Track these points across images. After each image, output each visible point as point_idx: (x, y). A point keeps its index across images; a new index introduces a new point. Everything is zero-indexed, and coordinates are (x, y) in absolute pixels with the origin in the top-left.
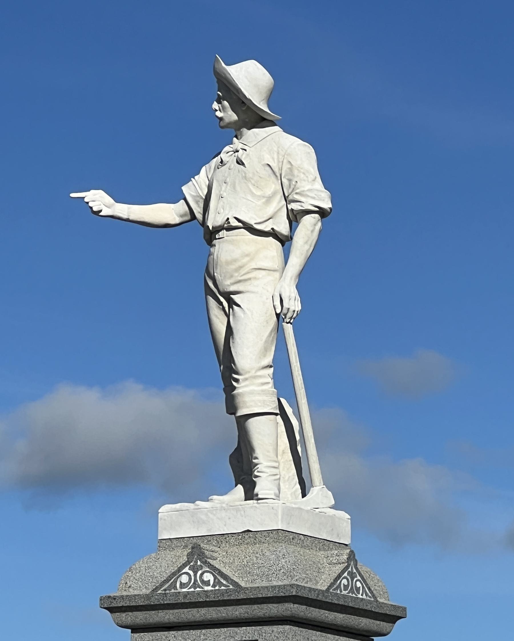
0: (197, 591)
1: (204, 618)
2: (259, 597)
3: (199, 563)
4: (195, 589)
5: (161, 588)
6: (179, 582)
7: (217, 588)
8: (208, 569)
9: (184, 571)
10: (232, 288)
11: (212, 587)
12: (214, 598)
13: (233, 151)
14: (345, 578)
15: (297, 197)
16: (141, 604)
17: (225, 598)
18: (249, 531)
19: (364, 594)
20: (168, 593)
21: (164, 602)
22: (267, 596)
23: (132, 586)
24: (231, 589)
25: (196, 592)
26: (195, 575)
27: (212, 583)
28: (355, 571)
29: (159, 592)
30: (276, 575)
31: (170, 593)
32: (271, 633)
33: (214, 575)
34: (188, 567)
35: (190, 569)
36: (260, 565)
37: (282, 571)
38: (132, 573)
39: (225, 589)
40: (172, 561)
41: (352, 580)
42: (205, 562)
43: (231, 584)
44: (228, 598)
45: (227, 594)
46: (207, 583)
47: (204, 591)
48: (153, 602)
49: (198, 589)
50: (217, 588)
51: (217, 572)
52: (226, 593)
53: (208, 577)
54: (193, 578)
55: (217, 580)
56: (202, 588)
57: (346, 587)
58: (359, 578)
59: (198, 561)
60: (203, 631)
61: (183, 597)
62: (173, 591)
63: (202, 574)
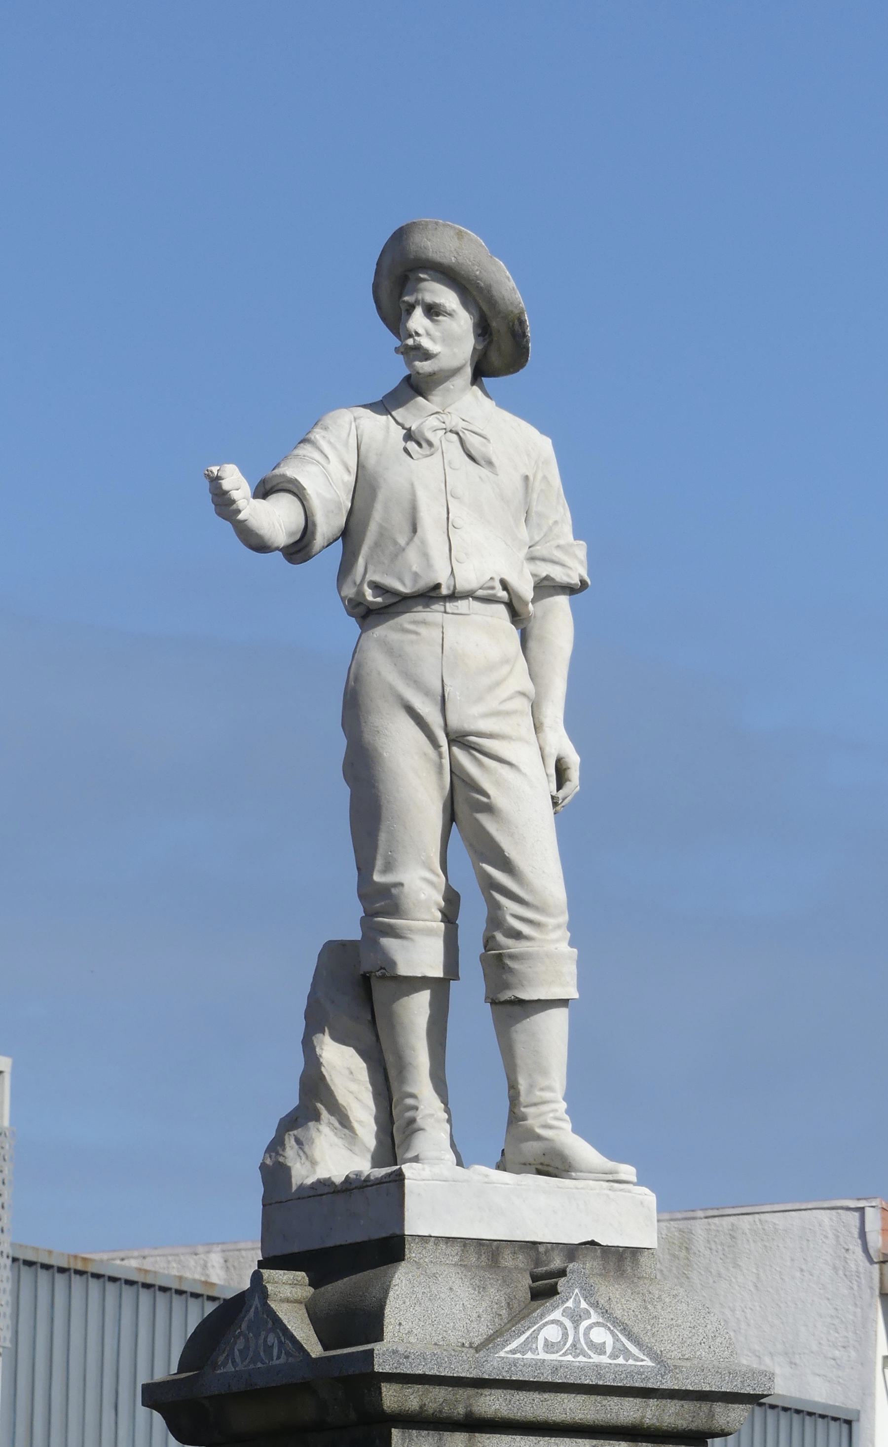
1: (569, 1418)
2: (704, 1389)
3: (584, 1305)
5: (504, 1346)
7: (621, 1361)
8: (601, 1320)
10: (483, 725)
11: (610, 1357)
12: (614, 1380)
13: (445, 429)
15: (558, 555)
16: (463, 1375)
17: (637, 1385)
18: (593, 1243)
21: (511, 1377)
22: (720, 1390)
25: (577, 1364)
27: (609, 1350)
29: (502, 1354)
30: (708, 1347)
31: (523, 1358)
34: (561, 1310)
35: (564, 1314)
37: (718, 1340)
42: (595, 1305)
43: (648, 1355)
44: (642, 1385)
45: (639, 1377)
46: (600, 1349)
52: (639, 1374)
53: (600, 1335)
54: (571, 1332)
56: (590, 1357)
60: (541, 1443)
61: (550, 1371)
62: (529, 1355)
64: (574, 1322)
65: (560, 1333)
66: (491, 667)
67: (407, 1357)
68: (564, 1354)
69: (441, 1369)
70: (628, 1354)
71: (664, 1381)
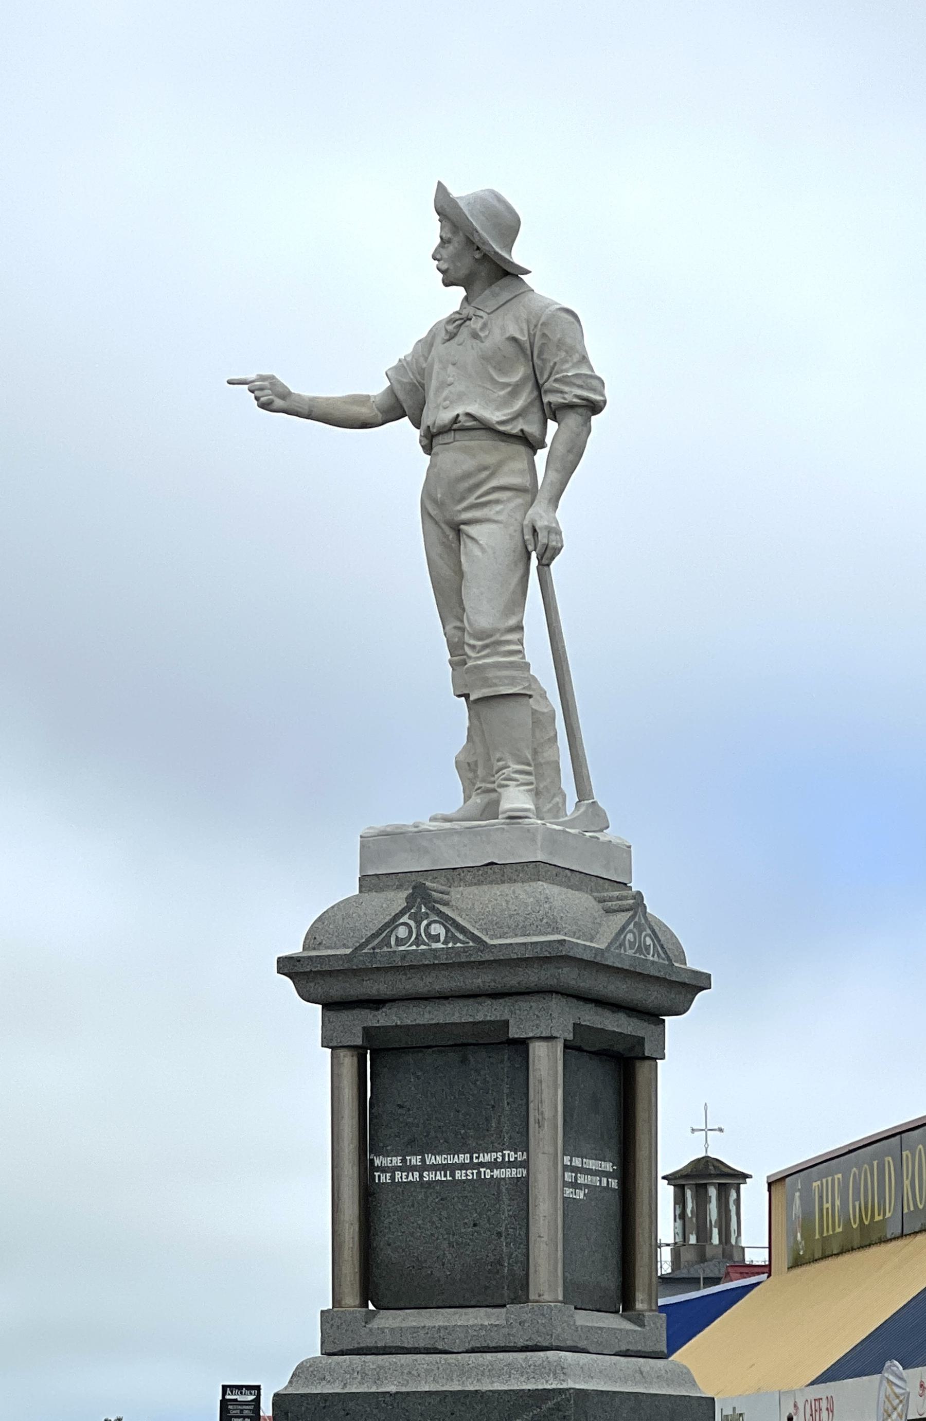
0: (421, 950)
4: (417, 947)
5: (367, 946)
6: (395, 937)
7: (450, 945)
8: (437, 918)
9: (401, 921)
10: (466, 516)
11: (443, 943)
14: (630, 931)
15: (557, 385)
17: (463, 960)
19: (656, 956)
20: (377, 953)
23: (324, 942)
24: (471, 946)
25: (420, 951)
26: (417, 926)
27: (442, 938)
28: (643, 921)
30: (535, 926)
32: (528, 1009)
33: (445, 927)
34: (407, 916)
36: (512, 913)
37: (545, 921)
38: (323, 923)
39: (461, 947)
40: (382, 907)
41: (640, 935)
42: (433, 909)
45: (465, 954)
46: (436, 938)
47: (431, 950)
48: (357, 966)
49: (423, 947)
50: (450, 945)
51: (450, 923)
54: (414, 931)
55: (449, 934)
57: (632, 944)
58: (649, 932)
59: (423, 906)
62: (385, 949)
63: (428, 925)
64: (416, 922)
65: (407, 931)
66: (467, 476)
67: (299, 961)
68: (410, 946)
69: (323, 967)
70: (458, 940)
71: (482, 956)
